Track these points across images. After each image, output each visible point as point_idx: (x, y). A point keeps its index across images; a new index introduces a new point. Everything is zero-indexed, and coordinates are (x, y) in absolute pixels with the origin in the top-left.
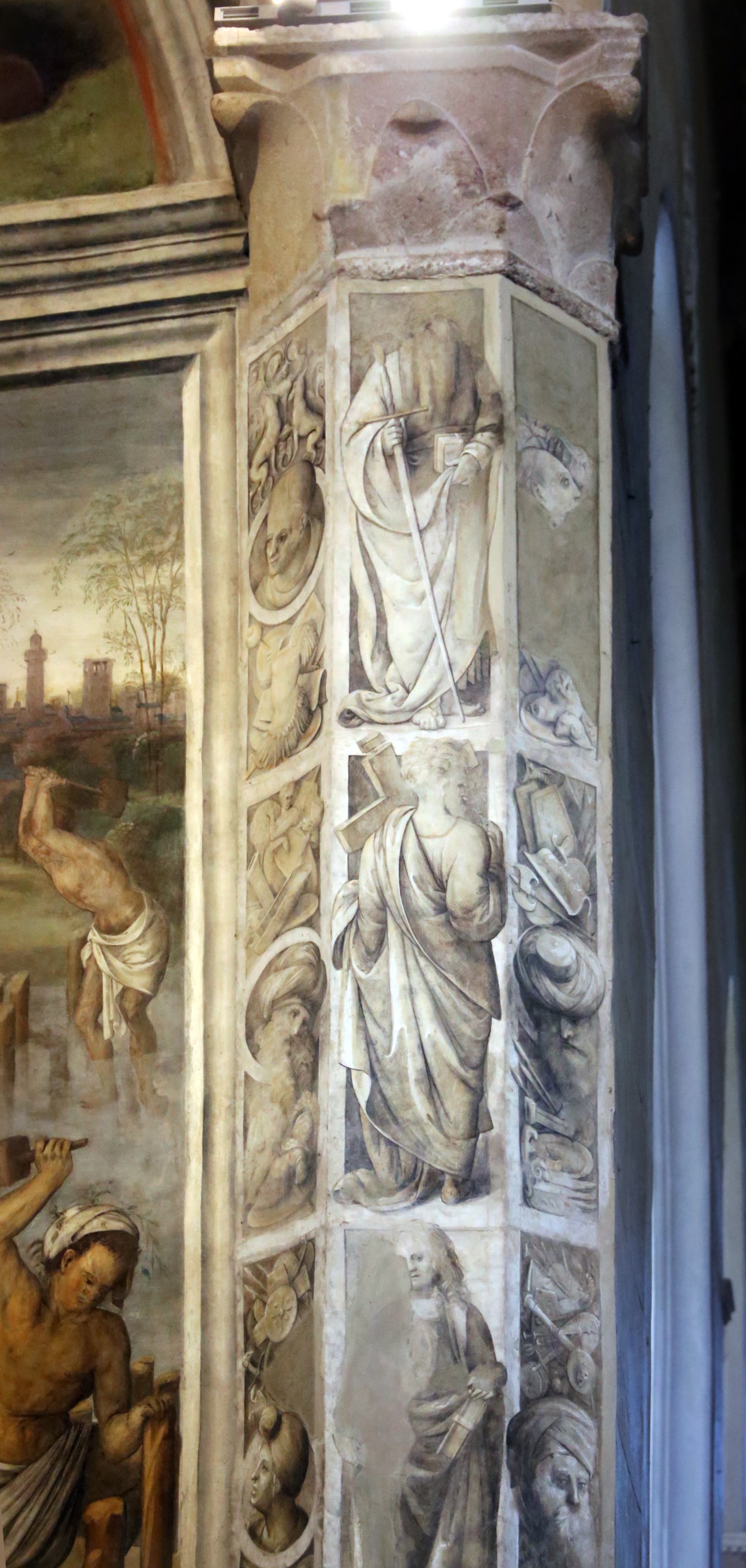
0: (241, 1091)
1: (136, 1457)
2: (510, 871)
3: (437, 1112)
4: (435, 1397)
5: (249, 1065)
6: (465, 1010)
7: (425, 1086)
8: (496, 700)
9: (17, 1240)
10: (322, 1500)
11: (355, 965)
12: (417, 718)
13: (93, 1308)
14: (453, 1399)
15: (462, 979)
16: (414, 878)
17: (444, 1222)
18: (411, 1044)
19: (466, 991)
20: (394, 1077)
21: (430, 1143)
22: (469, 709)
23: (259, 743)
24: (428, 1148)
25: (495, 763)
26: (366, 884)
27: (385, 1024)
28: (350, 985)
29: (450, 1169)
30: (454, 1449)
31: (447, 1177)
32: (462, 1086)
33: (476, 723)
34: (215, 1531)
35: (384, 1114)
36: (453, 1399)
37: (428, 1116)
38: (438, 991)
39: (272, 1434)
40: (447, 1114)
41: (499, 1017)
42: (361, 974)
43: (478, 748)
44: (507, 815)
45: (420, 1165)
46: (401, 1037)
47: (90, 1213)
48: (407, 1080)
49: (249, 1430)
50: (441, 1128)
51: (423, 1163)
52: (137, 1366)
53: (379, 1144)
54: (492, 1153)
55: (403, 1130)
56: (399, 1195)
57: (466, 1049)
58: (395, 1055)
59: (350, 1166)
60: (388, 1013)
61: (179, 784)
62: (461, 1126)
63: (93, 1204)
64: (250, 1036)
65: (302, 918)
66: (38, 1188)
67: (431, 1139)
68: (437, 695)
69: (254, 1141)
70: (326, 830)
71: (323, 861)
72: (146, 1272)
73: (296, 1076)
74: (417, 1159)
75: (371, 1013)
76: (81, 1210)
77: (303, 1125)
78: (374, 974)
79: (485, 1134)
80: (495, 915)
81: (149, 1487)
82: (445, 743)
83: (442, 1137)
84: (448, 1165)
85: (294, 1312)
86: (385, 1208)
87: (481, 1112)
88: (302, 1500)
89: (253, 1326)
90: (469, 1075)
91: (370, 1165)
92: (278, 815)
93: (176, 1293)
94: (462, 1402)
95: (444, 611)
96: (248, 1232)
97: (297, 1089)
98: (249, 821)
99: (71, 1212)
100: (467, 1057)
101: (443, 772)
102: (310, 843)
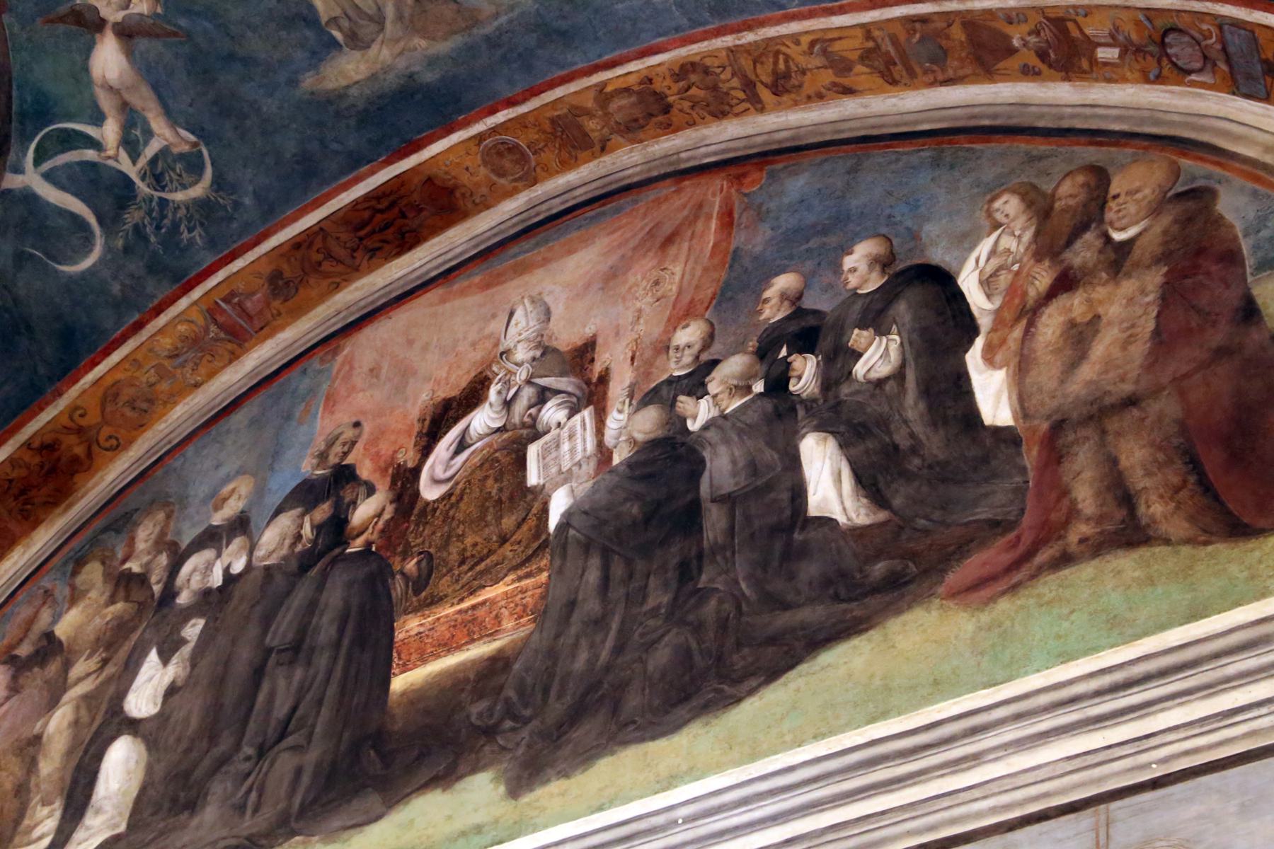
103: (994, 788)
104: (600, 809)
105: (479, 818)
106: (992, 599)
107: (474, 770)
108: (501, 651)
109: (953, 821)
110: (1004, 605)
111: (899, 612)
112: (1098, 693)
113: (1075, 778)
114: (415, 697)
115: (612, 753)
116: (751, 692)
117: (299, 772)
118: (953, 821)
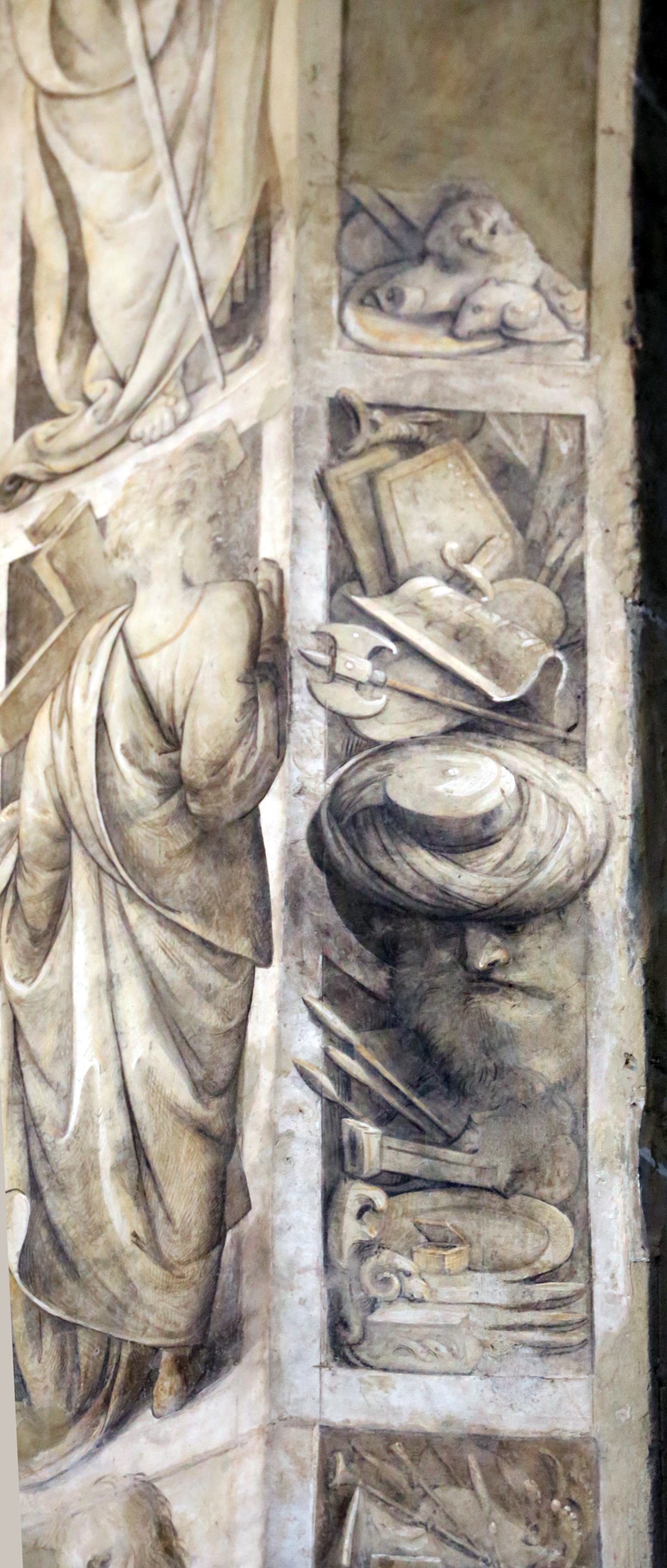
3: (150, 1221)
7: (129, 1176)
15: (205, 915)
16: (123, 747)
19: (211, 937)
20: (74, 1180)
21: (135, 1294)
24: (133, 1306)
27: (58, 1074)
29: (170, 1335)
31: (166, 1355)
32: (199, 1143)
35: (51, 1267)
37: (135, 1235)
38: (161, 960)
40: (169, 1218)
42: (20, 990)
45: (114, 1350)
46: (88, 1089)
48: (97, 1176)
51: (121, 1342)
53: (40, 1336)
54: (248, 1265)
55: (85, 1287)
57: (207, 1058)
58: (77, 1130)
62: (195, 1232)
67: (138, 1285)
74: (109, 1340)
75: (35, 1062)
79: (235, 1230)
80: (266, 748)
82: (188, 450)
83: (157, 1271)
84: (168, 1328)
86: (46, 1474)
87: (232, 1183)
95: (193, 191)
100: (209, 1075)
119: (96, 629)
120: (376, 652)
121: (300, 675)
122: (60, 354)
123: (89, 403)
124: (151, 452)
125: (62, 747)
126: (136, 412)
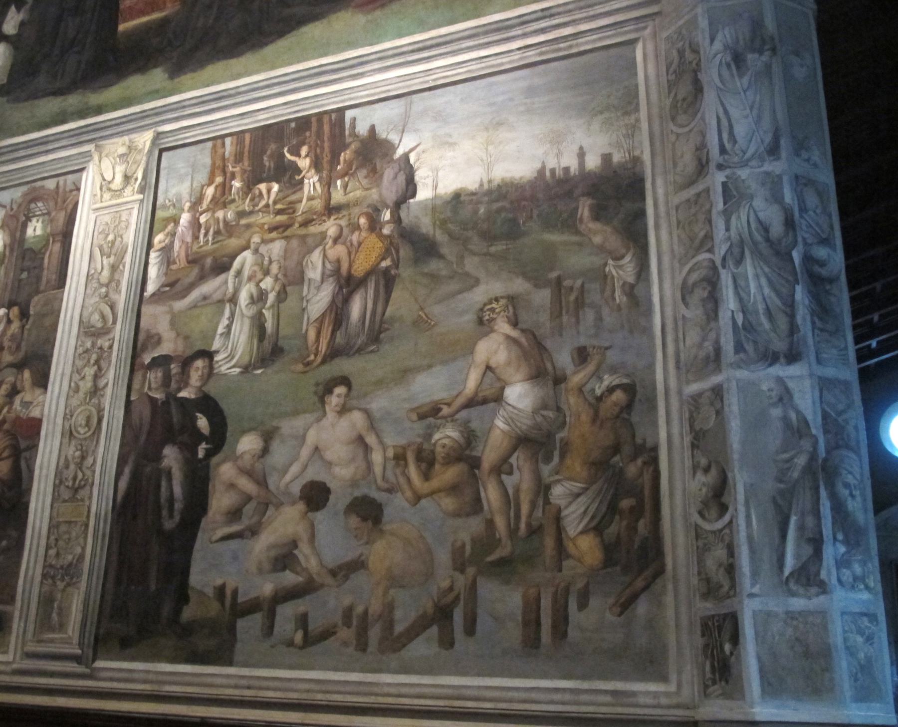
0: (680, 323)
1: (640, 480)
2: (797, 222)
4: (785, 452)
5: (683, 310)
6: (783, 282)
8: (784, 154)
9: (584, 389)
10: (735, 499)
11: (732, 266)
12: (750, 164)
13: (617, 417)
14: (793, 452)
15: (780, 269)
17: (781, 373)
18: (759, 298)
22: (772, 158)
23: (679, 179)
25: (785, 179)
26: (733, 232)
28: (730, 275)
30: (796, 475)
33: (775, 163)
34: (679, 511)
36: (793, 452)
39: (707, 470)
41: (798, 284)
42: (735, 271)
43: (778, 173)
44: (793, 200)
46: (754, 296)
47: (615, 376)
49: (695, 468)
50: (775, 332)
52: (639, 441)
56: (760, 364)
59: (737, 351)
60: (748, 286)
61: (644, 199)
63: (615, 373)
64: (683, 299)
65: (706, 248)
66: (591, 367)
68: (758, 153)
69: (689, 342)
70: (714, 211)
71: (713, 224)
72: (640, 400)
73: (708, 315)
75: (741, 287)
76: (610, 375)
77: (712, 335)
78: (740, 269)
81: (647, 492)
85: (714, 416)
88: (725, 499)
89: (694, 422)
90: (788, 310)
91: (745, 351)
92: (690, 208)
93: (653, 407)
94: (798, 453)
96: (688, 382)
97: (709, 320)
98: (677, 211)
99: (606, 377)
101: (763, 184)
102: (706, 218)
103: (368, 87)
104: (208, 86)
105: (158, 86)
106: (374, 9)
107: (155, 67)
108: (166, 16)
109: (351, 99)
110: (378, 13)
111: (335, 12)
112: (413, 51)
113: (400, 85)
114: (129, 34)
115: (213, 63)
116: (272, 42)
117: (79, 62)
118: (351, 99)
119: (744, 202)
120: (806, 226)
121: (798, 229)
122: (728, 142)
123: (737, 155)
124: (753, 170)
125: (739, 225)
126: (749, 160)
